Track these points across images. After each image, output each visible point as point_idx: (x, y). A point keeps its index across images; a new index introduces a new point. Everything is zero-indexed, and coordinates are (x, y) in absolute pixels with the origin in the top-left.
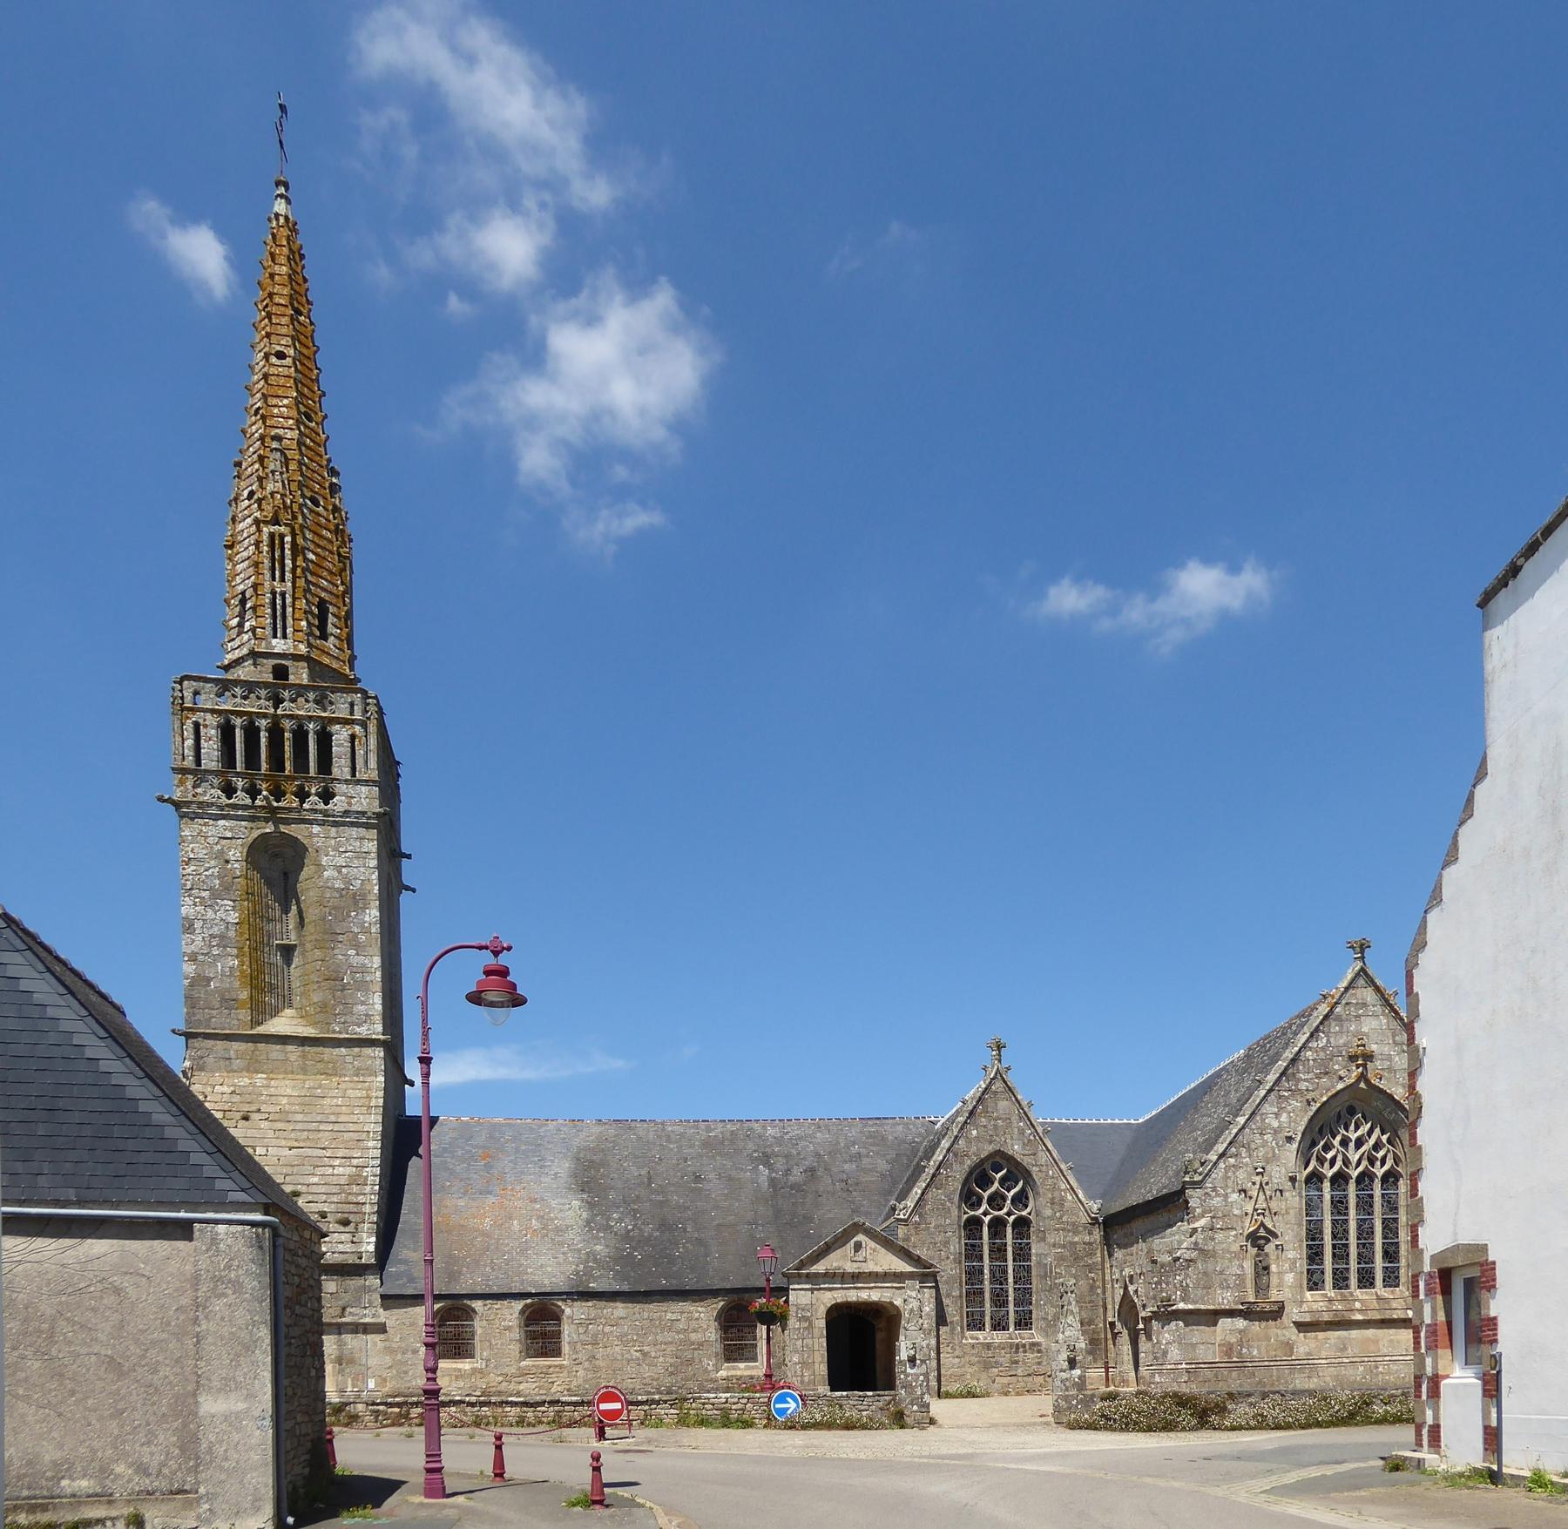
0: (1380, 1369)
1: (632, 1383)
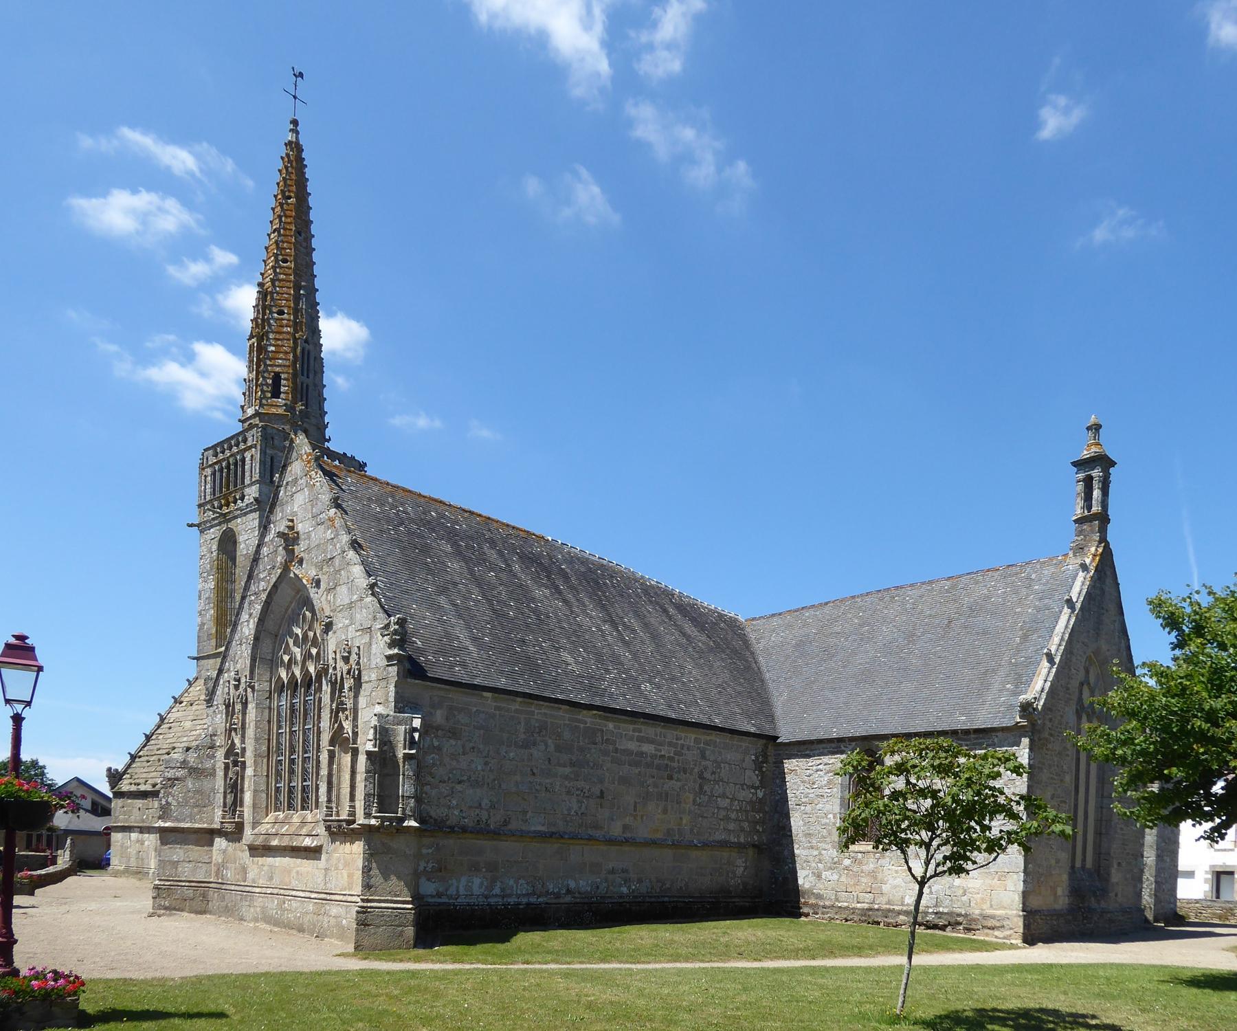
0: (286, 905)
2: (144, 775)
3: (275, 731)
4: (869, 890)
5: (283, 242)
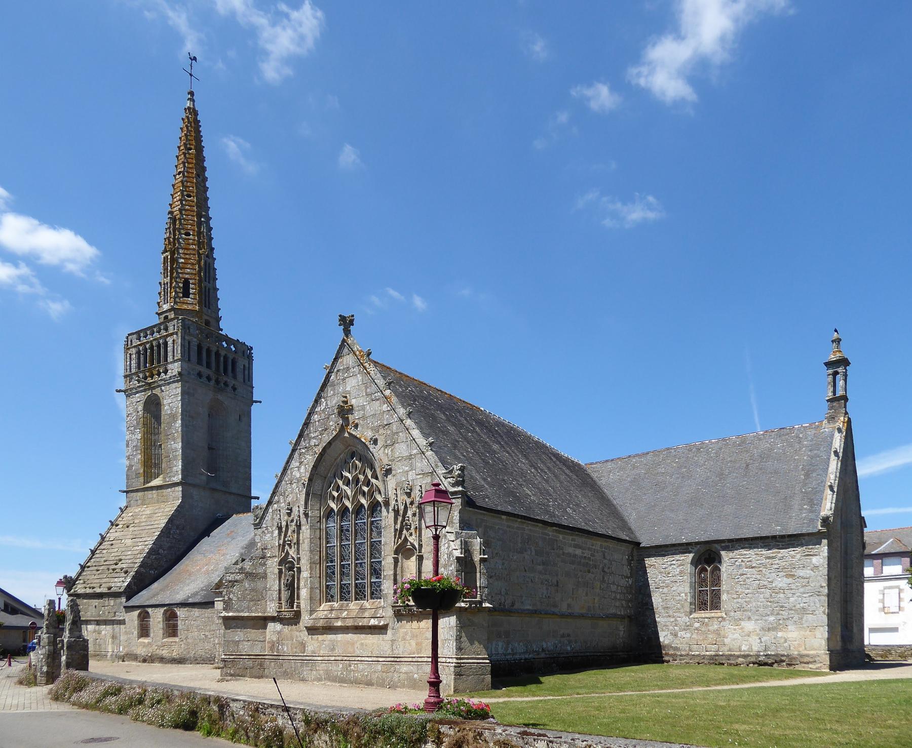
0: (352, 667)
1: (201, 652)
2: (97, 581)
3: (324, 545)
4: (714, 643)
5: (187, 182)
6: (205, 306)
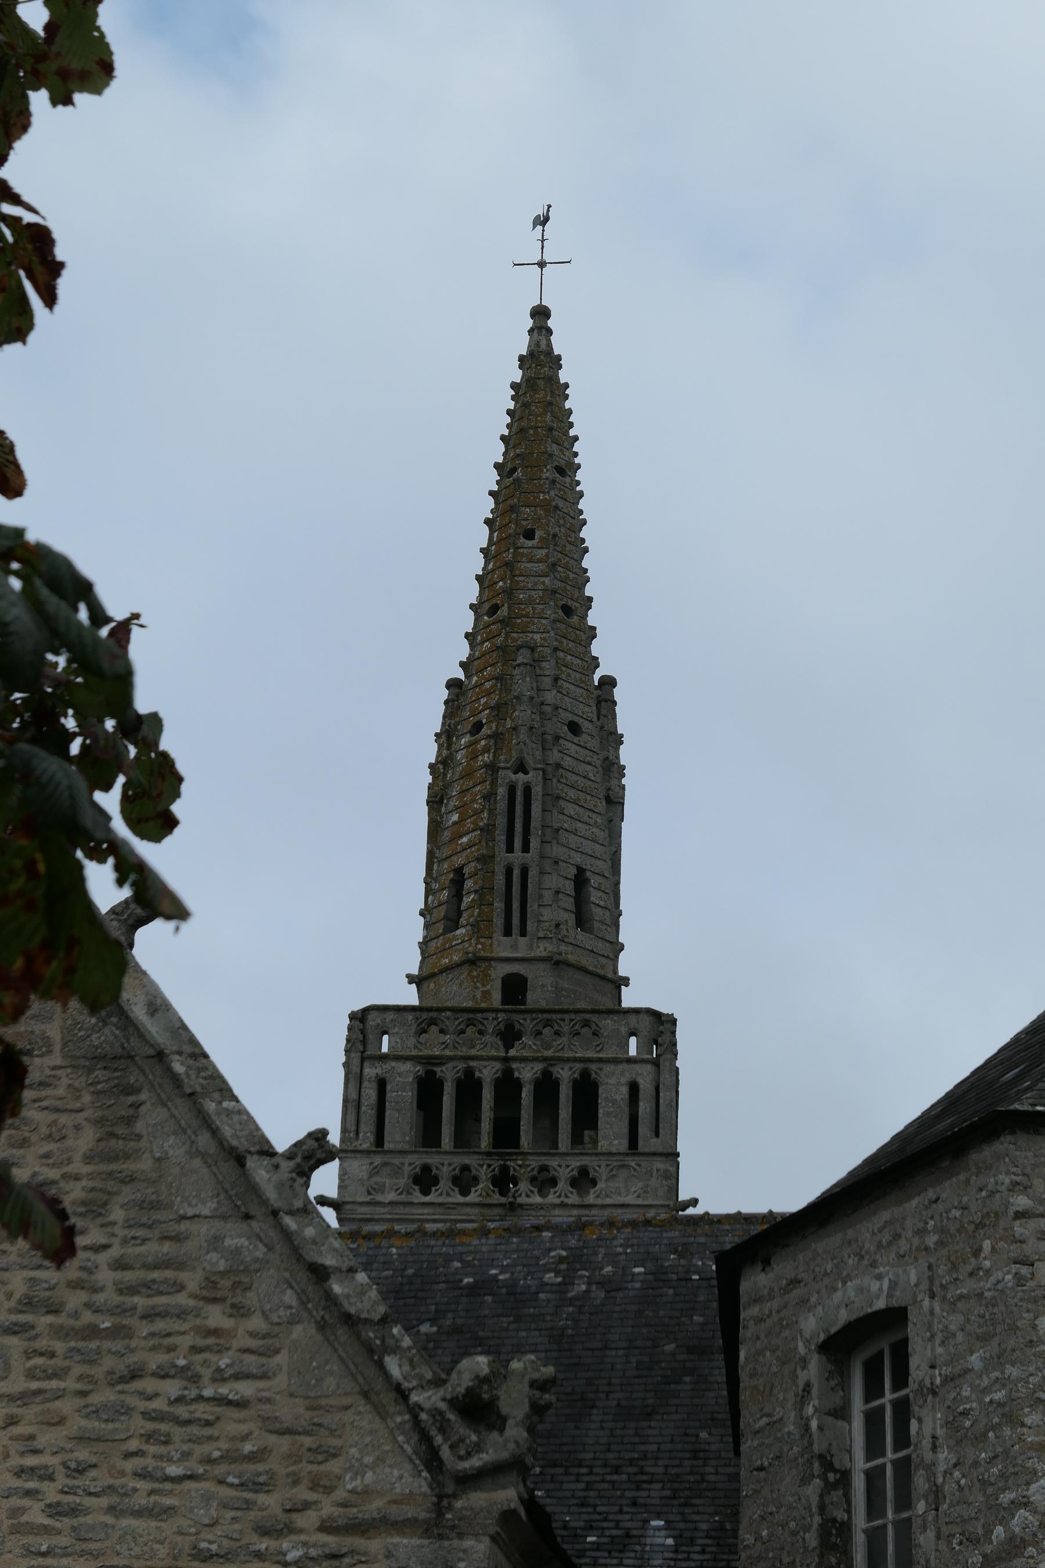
6: (508, 932)
